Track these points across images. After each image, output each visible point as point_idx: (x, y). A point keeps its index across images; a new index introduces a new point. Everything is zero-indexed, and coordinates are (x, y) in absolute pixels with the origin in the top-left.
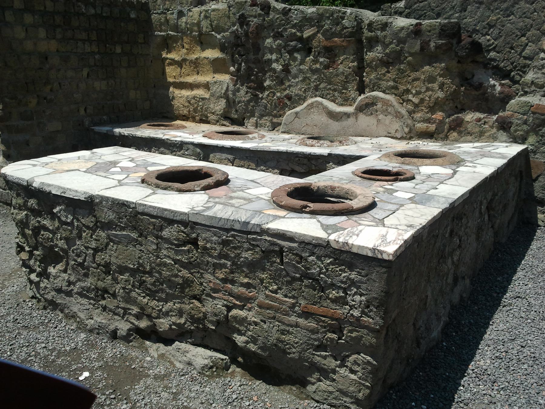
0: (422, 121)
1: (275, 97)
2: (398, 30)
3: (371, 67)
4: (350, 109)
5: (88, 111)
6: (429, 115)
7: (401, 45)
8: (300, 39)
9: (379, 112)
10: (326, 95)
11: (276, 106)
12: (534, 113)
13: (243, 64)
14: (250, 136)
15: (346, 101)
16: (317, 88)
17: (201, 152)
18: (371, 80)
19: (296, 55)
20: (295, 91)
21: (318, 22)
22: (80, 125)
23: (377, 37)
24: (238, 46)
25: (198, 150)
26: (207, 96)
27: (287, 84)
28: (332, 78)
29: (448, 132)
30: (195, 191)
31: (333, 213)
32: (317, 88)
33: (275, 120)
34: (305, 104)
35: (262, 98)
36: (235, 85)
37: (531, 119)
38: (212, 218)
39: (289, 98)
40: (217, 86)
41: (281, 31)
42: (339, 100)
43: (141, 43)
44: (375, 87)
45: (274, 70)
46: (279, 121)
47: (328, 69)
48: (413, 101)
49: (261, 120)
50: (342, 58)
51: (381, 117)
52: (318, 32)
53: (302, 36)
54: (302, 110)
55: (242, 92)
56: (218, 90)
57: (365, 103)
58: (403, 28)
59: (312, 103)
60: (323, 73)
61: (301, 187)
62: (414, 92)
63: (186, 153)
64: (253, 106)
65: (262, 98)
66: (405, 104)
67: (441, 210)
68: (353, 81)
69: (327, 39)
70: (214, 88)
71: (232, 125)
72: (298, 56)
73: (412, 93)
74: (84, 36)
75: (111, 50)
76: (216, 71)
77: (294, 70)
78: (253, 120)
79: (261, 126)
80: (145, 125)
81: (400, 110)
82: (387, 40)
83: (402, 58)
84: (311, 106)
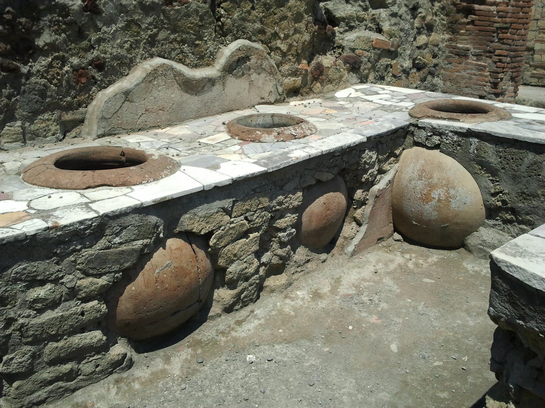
0: (289, 75)
1: (66, 68)
6: (296, 66)
9: (252, 70)
10: (170, 53)
11: (70, 87)
12: (374, 49)
15: (204, 59)
16: (152, 41)
18: (234, 21)
20: (110, 50)
25: (153, 219)
27: (94, 38)
28: (179, 20)
29: (312, 83)
32: (152, 41)
33: (68, 116)
35: (29, 75)
37: (373, 55)
39: (99, 65)
46: (78, 117)
48: (282, 48)
49: (32, 123)
51: (254, 76)
57: (237, 58)
59: (155, 70)
60: (164, 12)
62: (282, 36)
63: (117, 240)
64: (9, 97)
65: (29, 75)
68: (210, 24)
73: (280, 38)
84: (153, 75)
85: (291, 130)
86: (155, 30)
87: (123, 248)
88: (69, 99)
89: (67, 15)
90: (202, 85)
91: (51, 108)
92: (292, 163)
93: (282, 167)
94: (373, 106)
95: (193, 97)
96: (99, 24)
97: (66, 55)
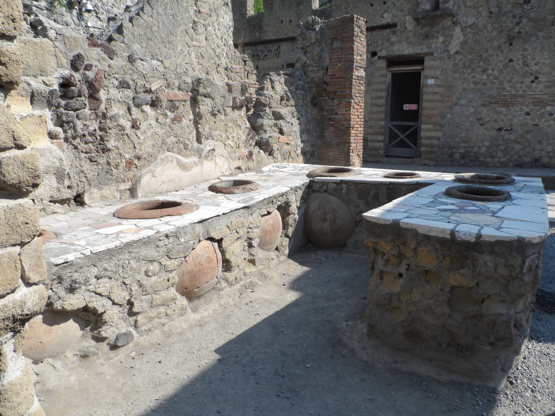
21: (163, 75)
32: (164, 142)
34: (158, 161)
44: (209, 137)
77: (144, 126)
85: (249, 186)
94: (286, 174)
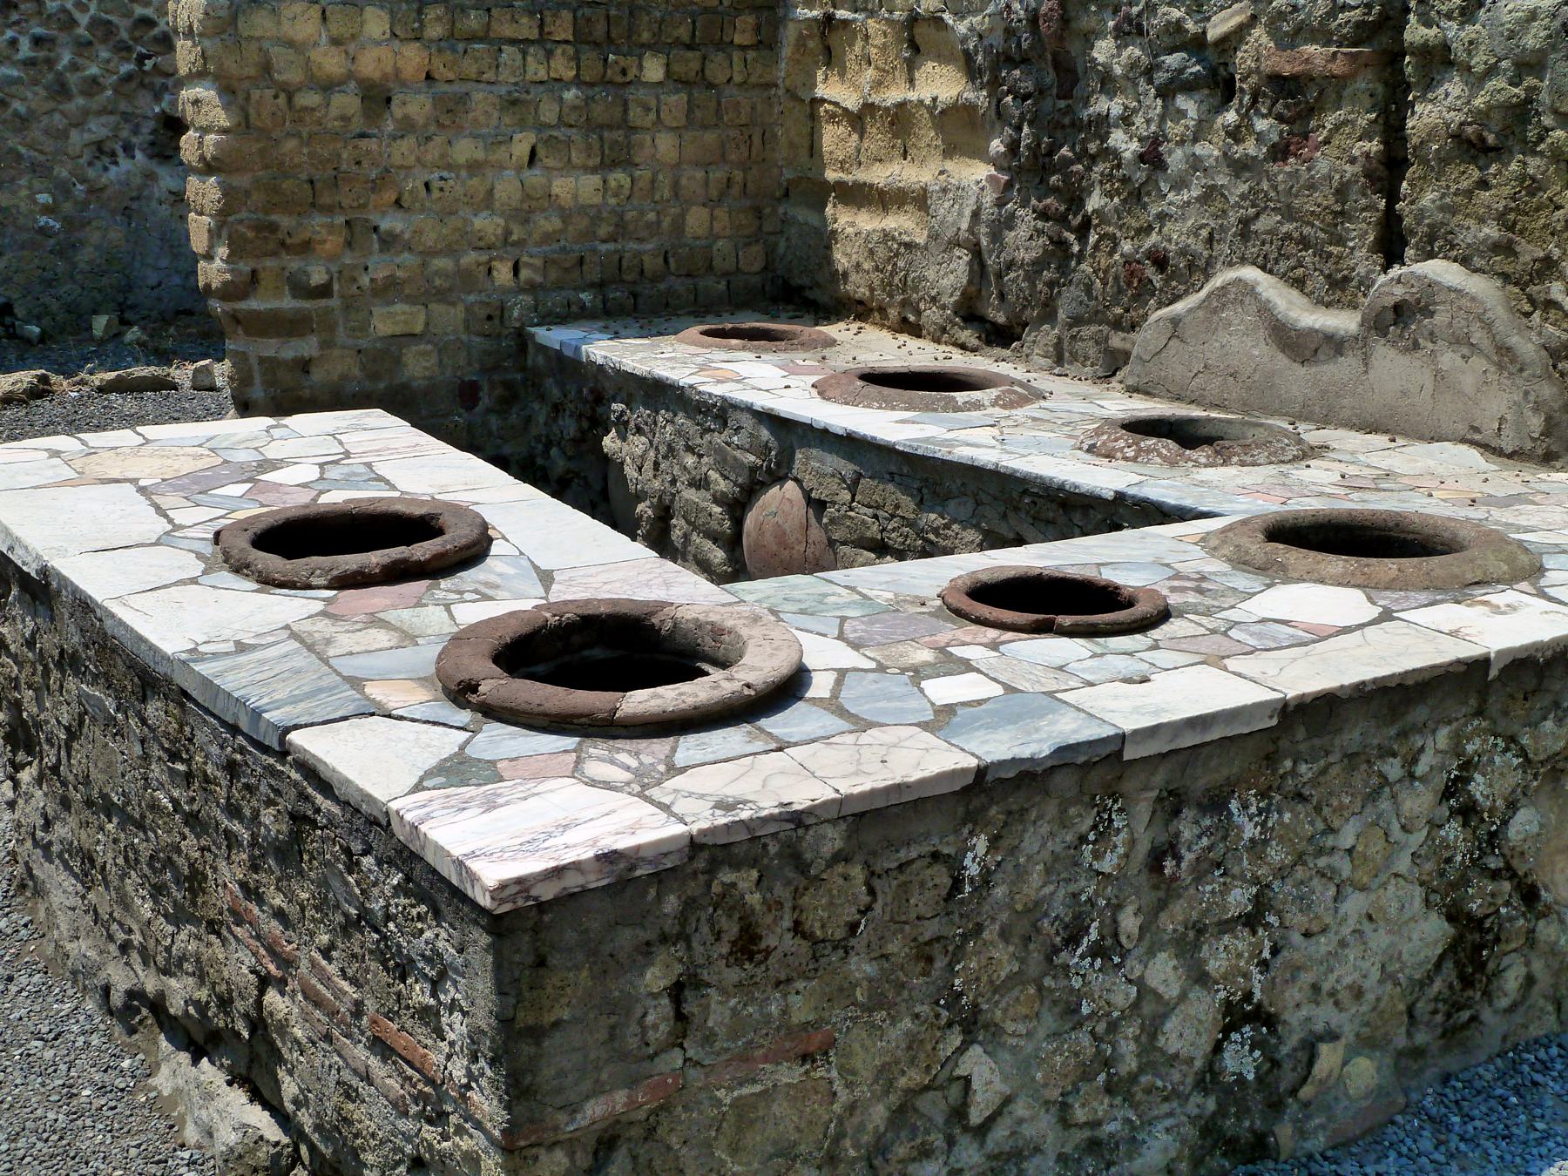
1: (1117, 257)
2: (1518, 22)
3: (1425, 162)
4: (1344, 322)
5: (525, 274)
7: (1530, 81)
8: (1197, 45)
11: (1120, 291)
13: (1026, 129)
14: (961, 397)
15: (1339, 289)
17: (773, 443)
19: (1182, 102)
20: (1177, 236)
22: (490, 318)
23: (1446, 47)
24: (1010, 61)
25: (765, 434)
26: (921, 239)
30: (309, 587)
31: (545, 724)
33: (1117, 340)
35: (1080, 257)
36: (1000, 203)
38: (206, 682)
39: (1160, 262)
40: (947, 204)
41: (1140, 15)
42: (1317, 282)
43: (743, 48)
45: (1115, 154)
47: (1285, 159)
50: (1330, 119)
51: (1449, 359)
52: (1254, 18)
53: (1204, 33)
54: (1190, 311)
55: (1021, 232)
56: (950, 219)
58: (1533, 15)
61: (610, 616)
64: (1051, 284)
66: (1537, 316)
67: (973, 763)
69: (1280, 46)
70: (942, 208)
71: (989, 343)
72: (1188, 105)
74: (526, 28)
75: (624, 72)
76: (950, 151)
77: (1176, 159)
78: (1047, 335)
79: (1074, 357)
80: (694, 331)
81: (1514, 340)
82: (1479, 61)
83: (1532, 134)
86: (1251, 211)
87: (738, 453)
88: (1119, 311)
89: (1119, 166)
90: (1313, 346)
91: (1096, 317)
92: (949, 458)
93: (920, 452)
95: (1296, 366)
96: (1165, 187)
97: (1119, 234)
